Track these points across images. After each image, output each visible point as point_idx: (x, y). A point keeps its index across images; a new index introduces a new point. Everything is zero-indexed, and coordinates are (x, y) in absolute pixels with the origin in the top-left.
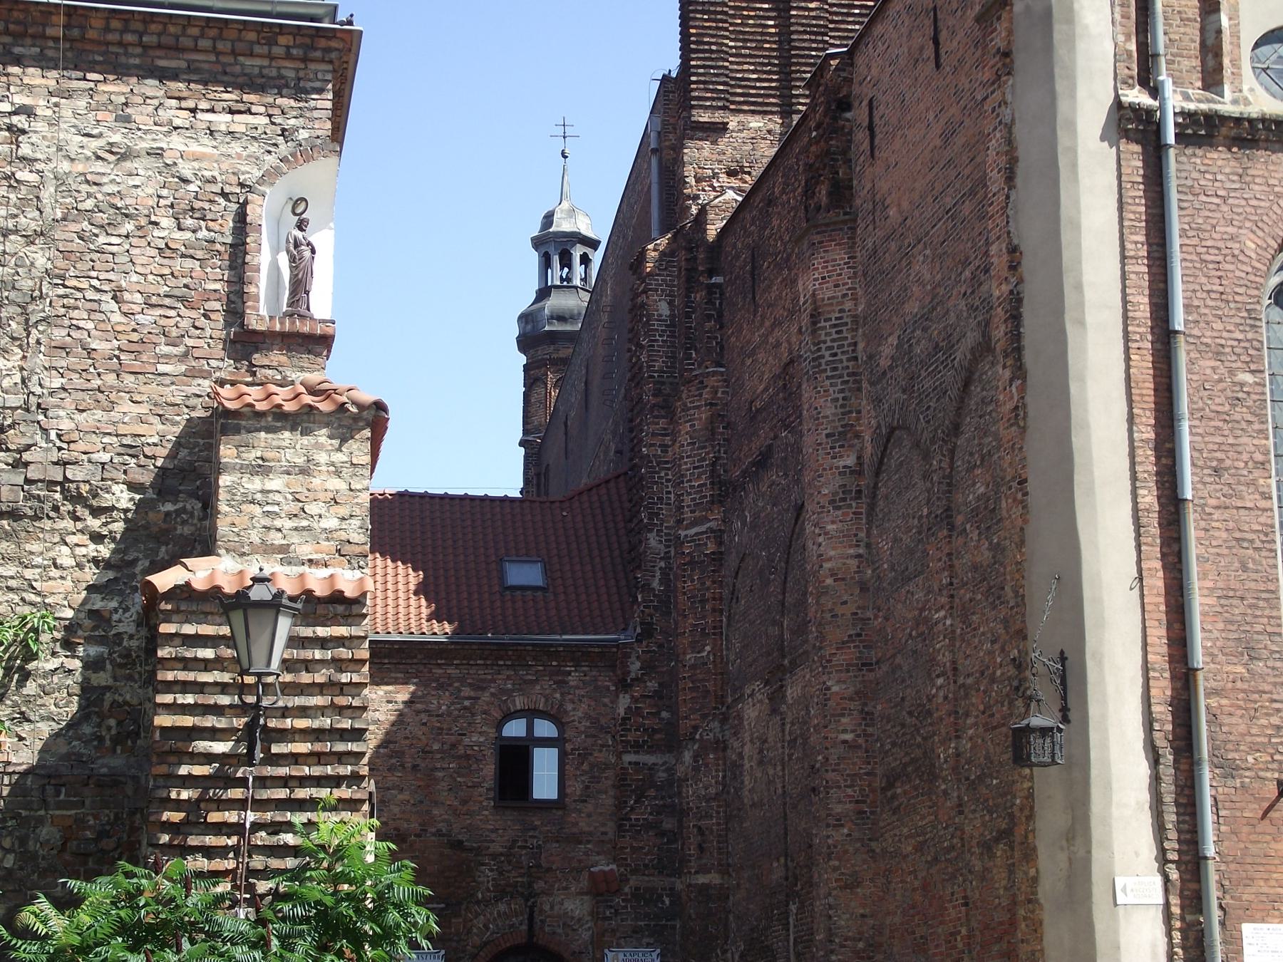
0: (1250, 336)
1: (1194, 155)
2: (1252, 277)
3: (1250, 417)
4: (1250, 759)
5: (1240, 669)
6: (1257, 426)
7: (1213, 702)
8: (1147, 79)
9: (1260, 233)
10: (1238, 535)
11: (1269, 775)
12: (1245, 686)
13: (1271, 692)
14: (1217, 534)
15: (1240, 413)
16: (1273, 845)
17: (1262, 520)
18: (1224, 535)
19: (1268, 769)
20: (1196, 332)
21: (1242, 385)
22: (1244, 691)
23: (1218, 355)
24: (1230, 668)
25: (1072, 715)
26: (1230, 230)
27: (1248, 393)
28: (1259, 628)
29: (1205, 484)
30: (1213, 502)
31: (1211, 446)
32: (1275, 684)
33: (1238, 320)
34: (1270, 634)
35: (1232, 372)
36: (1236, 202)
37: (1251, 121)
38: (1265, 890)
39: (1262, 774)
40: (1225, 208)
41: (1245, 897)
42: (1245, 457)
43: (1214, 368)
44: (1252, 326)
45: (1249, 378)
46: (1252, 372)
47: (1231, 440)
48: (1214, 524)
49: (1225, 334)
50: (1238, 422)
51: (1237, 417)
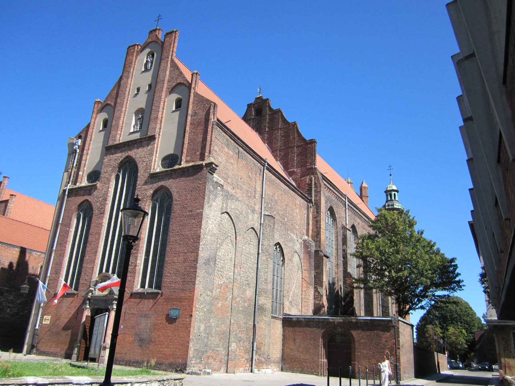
7: (50, 281)
35: (66, 228)
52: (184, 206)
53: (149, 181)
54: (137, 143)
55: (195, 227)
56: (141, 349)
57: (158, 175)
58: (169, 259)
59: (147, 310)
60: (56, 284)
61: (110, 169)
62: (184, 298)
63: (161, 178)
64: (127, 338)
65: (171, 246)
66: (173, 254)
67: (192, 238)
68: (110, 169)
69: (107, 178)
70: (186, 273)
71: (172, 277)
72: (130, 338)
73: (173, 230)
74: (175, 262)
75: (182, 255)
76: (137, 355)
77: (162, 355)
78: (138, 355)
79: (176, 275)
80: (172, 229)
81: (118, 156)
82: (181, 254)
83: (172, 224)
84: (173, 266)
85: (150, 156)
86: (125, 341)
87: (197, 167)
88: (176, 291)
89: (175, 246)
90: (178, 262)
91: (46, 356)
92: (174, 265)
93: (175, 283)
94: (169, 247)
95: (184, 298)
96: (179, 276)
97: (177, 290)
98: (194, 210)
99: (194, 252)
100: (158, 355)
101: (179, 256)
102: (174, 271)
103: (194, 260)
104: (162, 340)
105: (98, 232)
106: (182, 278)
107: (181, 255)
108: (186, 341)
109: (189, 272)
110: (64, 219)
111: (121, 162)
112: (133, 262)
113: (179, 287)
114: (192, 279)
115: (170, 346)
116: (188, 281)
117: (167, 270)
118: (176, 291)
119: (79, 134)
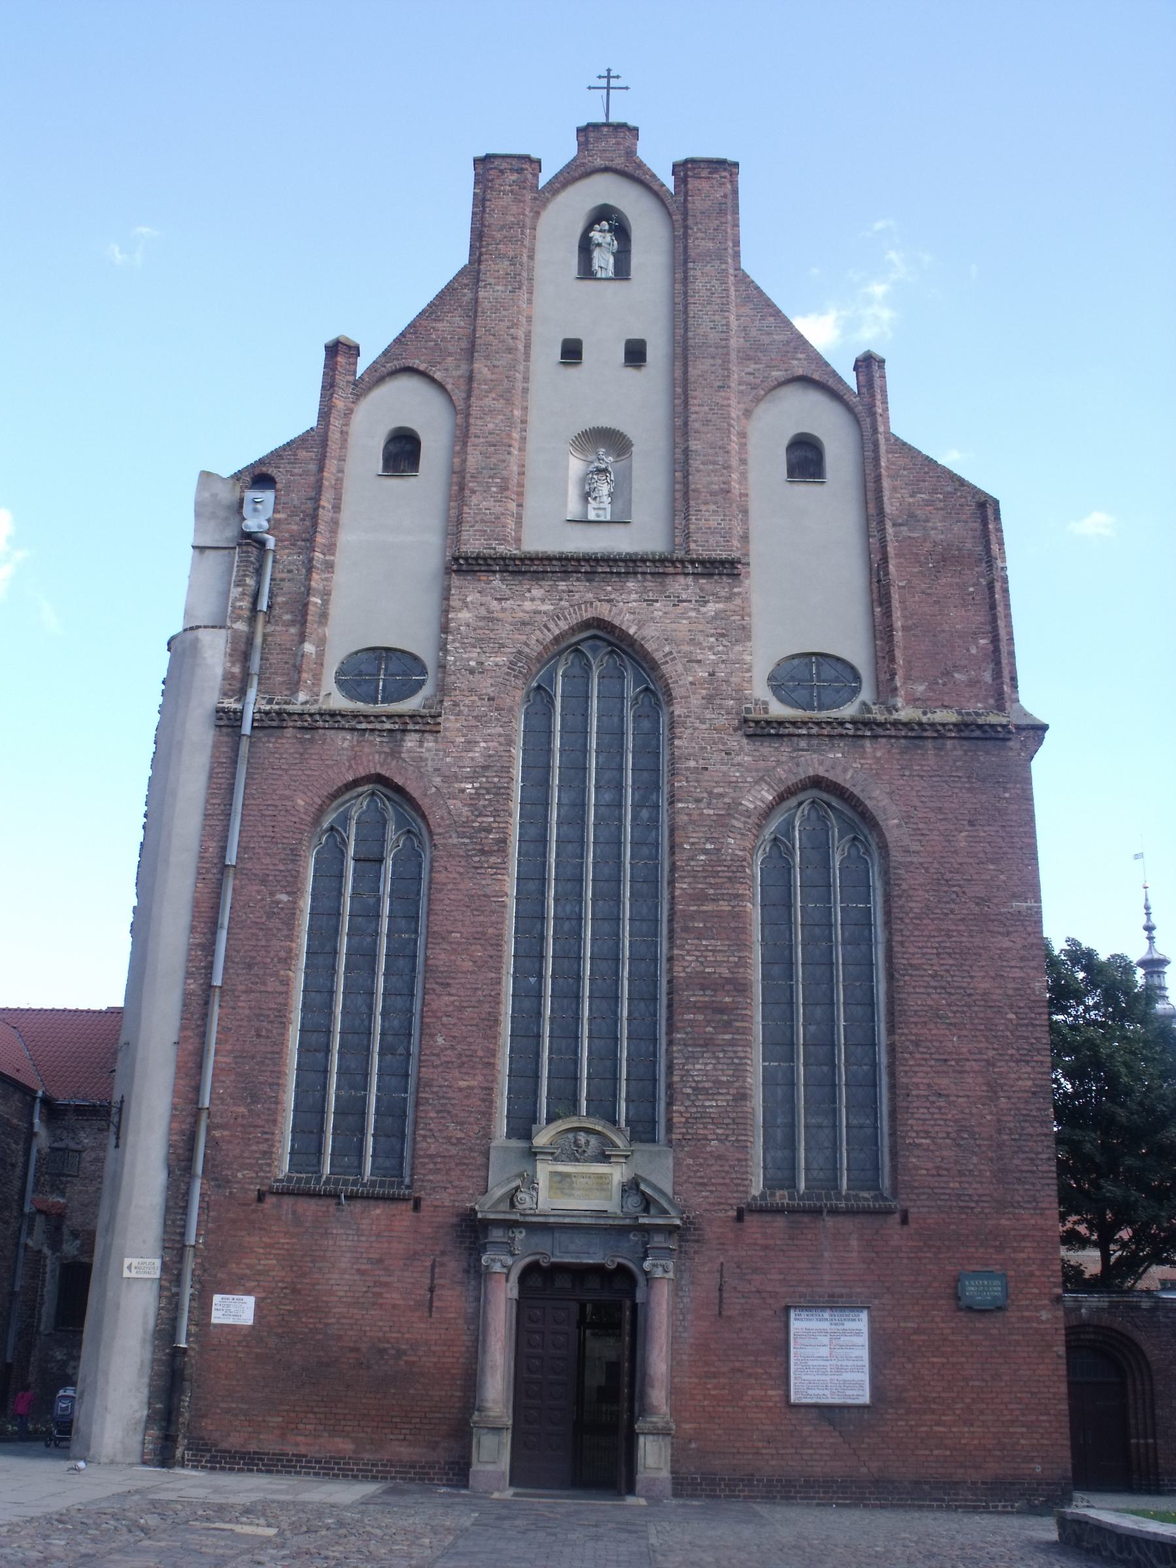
0: (290, 867)
1: (269, 742)
2: (297, 825)
3: (280, 926)
4: (240, 1175)
5: (242, 1110)
6: (285, 932)
7: (217, 1134)
8: (242, 693)
9: (309, 794)
10: (257, 1011)
11: (252, 1187)
12: (245, 1122)
13: (263, 1127)
14: (241, 1011)
15: (275, 923)
16: (248, 1239)
17: (278, 1000)
18: (247, 1012)
19: (251, 1183)
20: (249, 866)
21: (278, 902)
22: (243, 1126)
23: (263, 882)
24: (235, 1109)
25: (121, 1144)
26: (287, 792)
27: (282, 909)
28: (261, 1079)
29: (238, 975)
30: (242, 987)
31: (247, 948)
32: (267, 1121)
33: (283, 856)
34: (270, 1084)
35: (272, 894)
36: (295, 772)
37: (311, 715)
38: (237, 1271)
39: (247, 1186)
40: (286, 777)
41: (219, 1275)
42: (272, 954)
43: (259, 892)
44: (293, 861)
45: (284, 898)
46: (288, 893)
47: (263, 943)
48: (240, 1004)
49: (271, 867)
50: (271, 929)
51: (271, 925)
52: (948, 876)
53: (742, 749)
54: (635, 573)
55: (1013, 963)
56: (837, 1434)
57: (791, 730)
58: (915, 1080)
59: (837, 1278)
60: (264, 1147)
61: (501, 659)
62: (1013, 1233)
63: (803, 744)
64: (750, 1392)
65: (914, 1031)
66: (933, 1063)
67: (1011, 1007)
68: (501, 659)
69: (491, 699)
70: (1006, 1137)
71: (945, 1153)
72: (770, 1392)
73: (911, 965)
74: (947, 1096)
75: (977, 1068)
76: (817, 1457)
77: (948, 1453)
78: (825, 1458)
79: (959, 1145)
80: (905, 962)
81: (540, 612)
82: (968, 1066)
83: (902, 943)
84: (940, 1108)
85: (725, 643)
86: (742, 1403)
87: (978, 733)
88: (973, 1205)
89: (934, 1032)
90: (961, 1093)
91: (269, 1471)
92: (942, 1104)
93: (961, 1173)
94: (906, 1031)
95: (1013, 1233)
96: (976, 1149)
97: (977, 1202)
98: (995, 901)
99: (1027, 1062)
100: (927, 1452)
101: (960, 1072)
102: (950, 1129)
103: (1034, 1093)
104: (934, 1395)
105: (483, 933)
106: (991, 1160)
107: (968, 1069)
108: (1051, 1396)
109: (1020, 1135)
110: (245, 848)
111: (557, 640)
112: (724, 1079)
113: (980, 1192)
114: (1039, 1162)
115: (981, 1418)
116: (1022, 1171)
117: (910, 1122)
118: (972, 1208)
119: (261, 462)
